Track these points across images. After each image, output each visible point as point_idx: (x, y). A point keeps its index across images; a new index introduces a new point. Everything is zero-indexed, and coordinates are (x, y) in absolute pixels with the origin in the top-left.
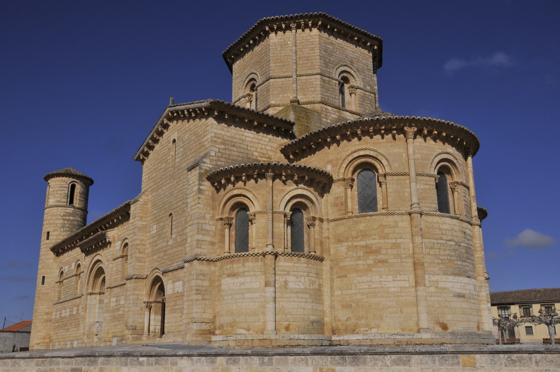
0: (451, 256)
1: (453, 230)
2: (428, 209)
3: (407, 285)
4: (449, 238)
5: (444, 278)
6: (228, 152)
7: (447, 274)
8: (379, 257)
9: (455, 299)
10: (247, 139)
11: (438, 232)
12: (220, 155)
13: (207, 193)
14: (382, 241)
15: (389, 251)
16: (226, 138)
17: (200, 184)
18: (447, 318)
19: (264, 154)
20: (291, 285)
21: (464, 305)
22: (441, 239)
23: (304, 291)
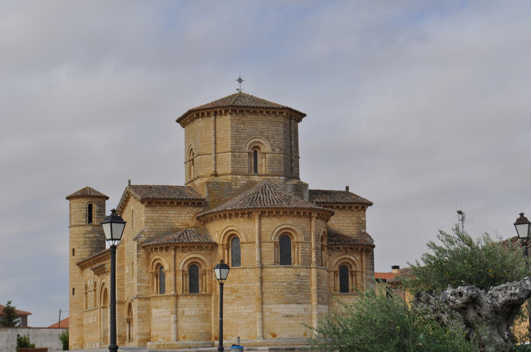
0: (283, 292)
1: (287, 275)
2: (268, 264)
3: (252, 311)
4: (283, 281)
5: (276, 306)
6: (156, 227)
7: (278, 304)
8: (238, 295)
9: (284, 318)
10: (171, 215)
11: (274, 277)
12: (151, 230)
13: (143, 256)
14: (240, 285)
15: (243, 291)
16: (155, 218)
17: (138, 252)
18: (277, 331)
19: (183, 223)
20: (186, 313)
21: (290, 322)
22: (276, 282)
23: (196, 316)
